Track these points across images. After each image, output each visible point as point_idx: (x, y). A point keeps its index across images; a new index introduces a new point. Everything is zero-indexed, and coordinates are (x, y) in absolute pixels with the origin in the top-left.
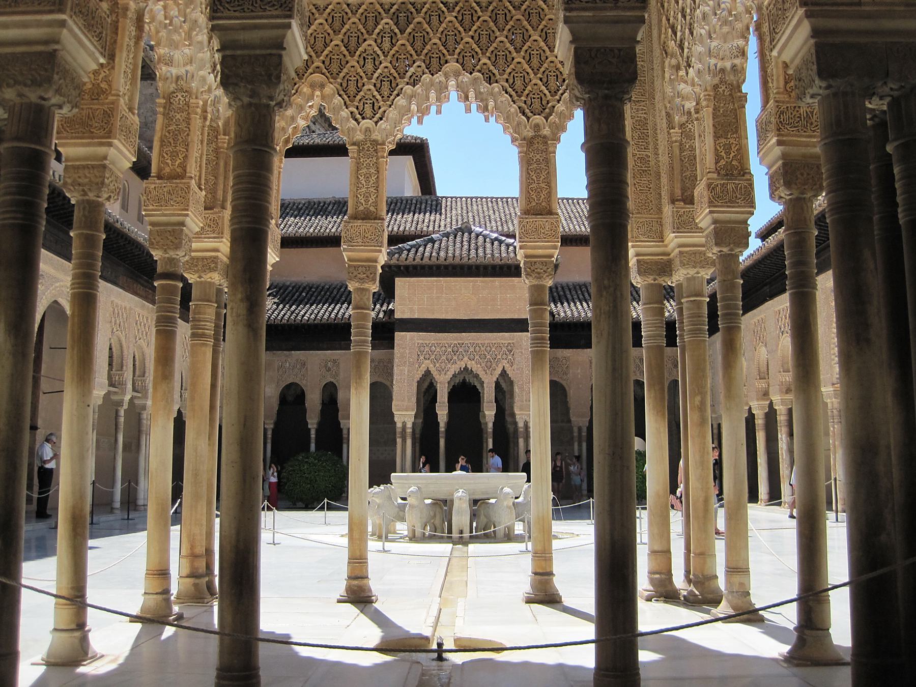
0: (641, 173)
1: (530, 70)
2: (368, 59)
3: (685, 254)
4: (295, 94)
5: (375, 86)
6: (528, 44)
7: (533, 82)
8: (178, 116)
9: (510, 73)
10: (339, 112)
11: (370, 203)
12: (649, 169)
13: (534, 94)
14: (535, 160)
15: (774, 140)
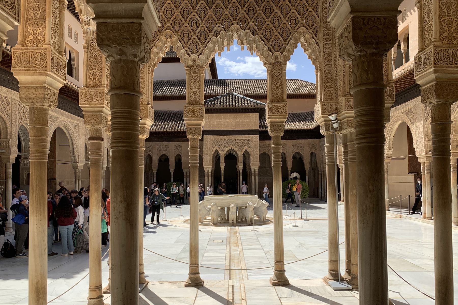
0: (328, 80)
1: (274, 28)
2: (193, 22)
3: (350, 121)
4: (158, 41)
5: (197, 36)
6: (273, 14)
7: (275, 34)
8: (95, 53)
9: (264, 30)
10: (180, 51)
11: (196, 96)
12: (332, 78)
13: (275, 41)
14: (276, 75)
15: (432, 70)
